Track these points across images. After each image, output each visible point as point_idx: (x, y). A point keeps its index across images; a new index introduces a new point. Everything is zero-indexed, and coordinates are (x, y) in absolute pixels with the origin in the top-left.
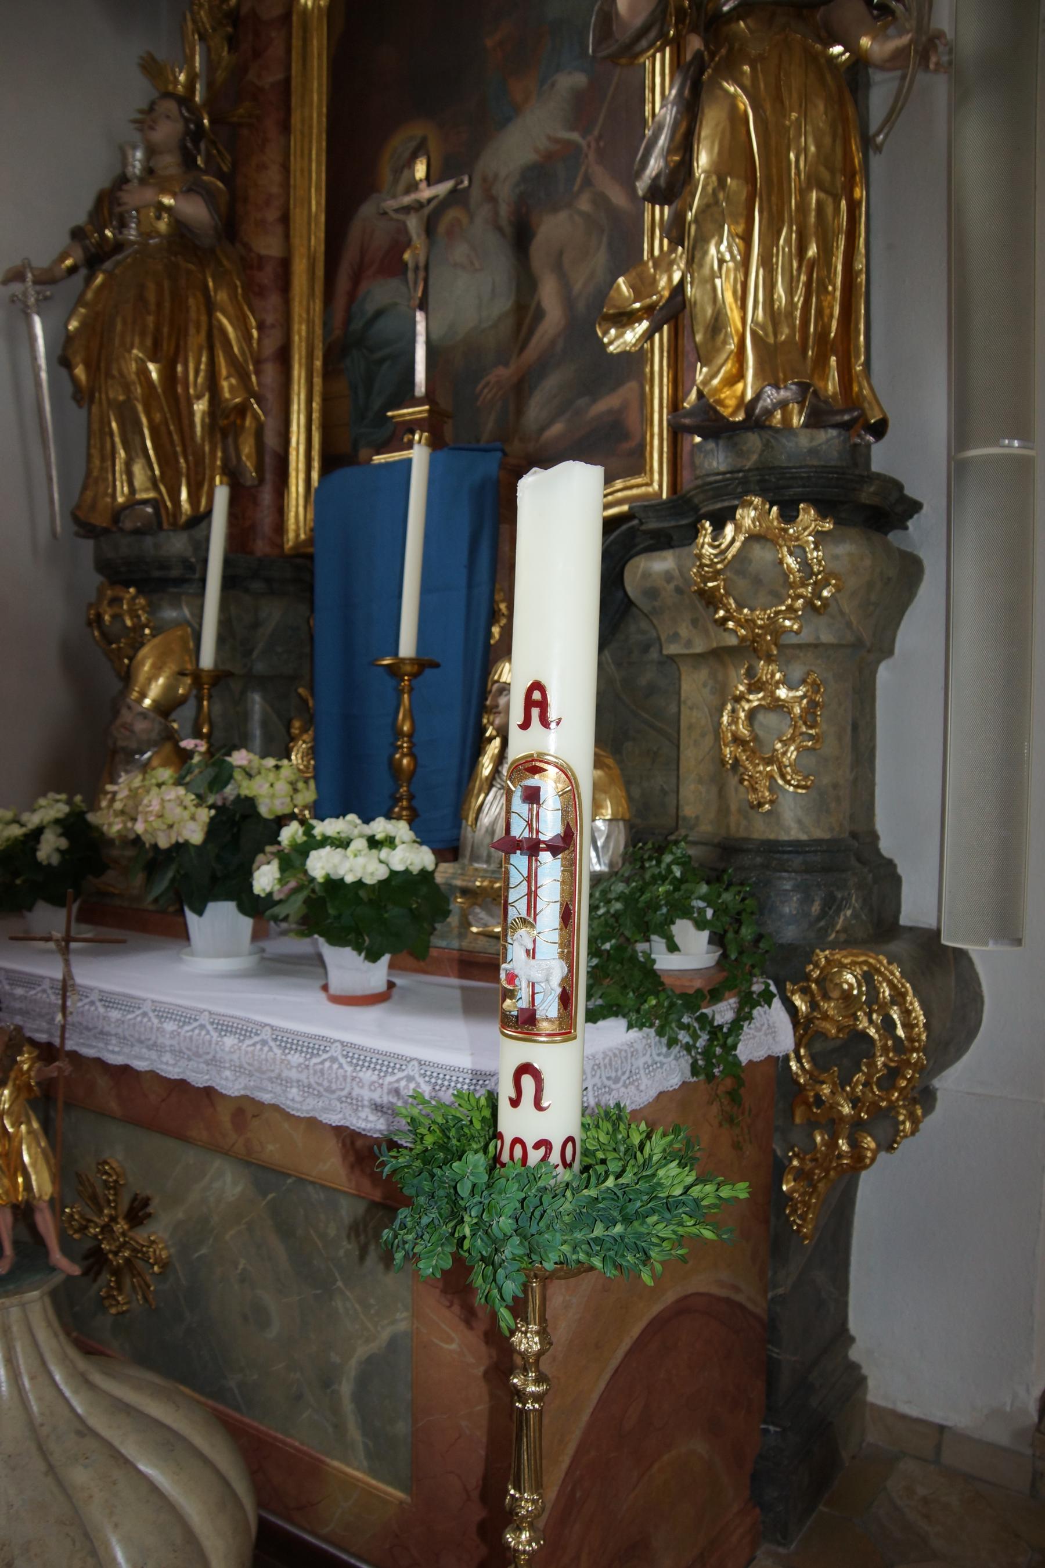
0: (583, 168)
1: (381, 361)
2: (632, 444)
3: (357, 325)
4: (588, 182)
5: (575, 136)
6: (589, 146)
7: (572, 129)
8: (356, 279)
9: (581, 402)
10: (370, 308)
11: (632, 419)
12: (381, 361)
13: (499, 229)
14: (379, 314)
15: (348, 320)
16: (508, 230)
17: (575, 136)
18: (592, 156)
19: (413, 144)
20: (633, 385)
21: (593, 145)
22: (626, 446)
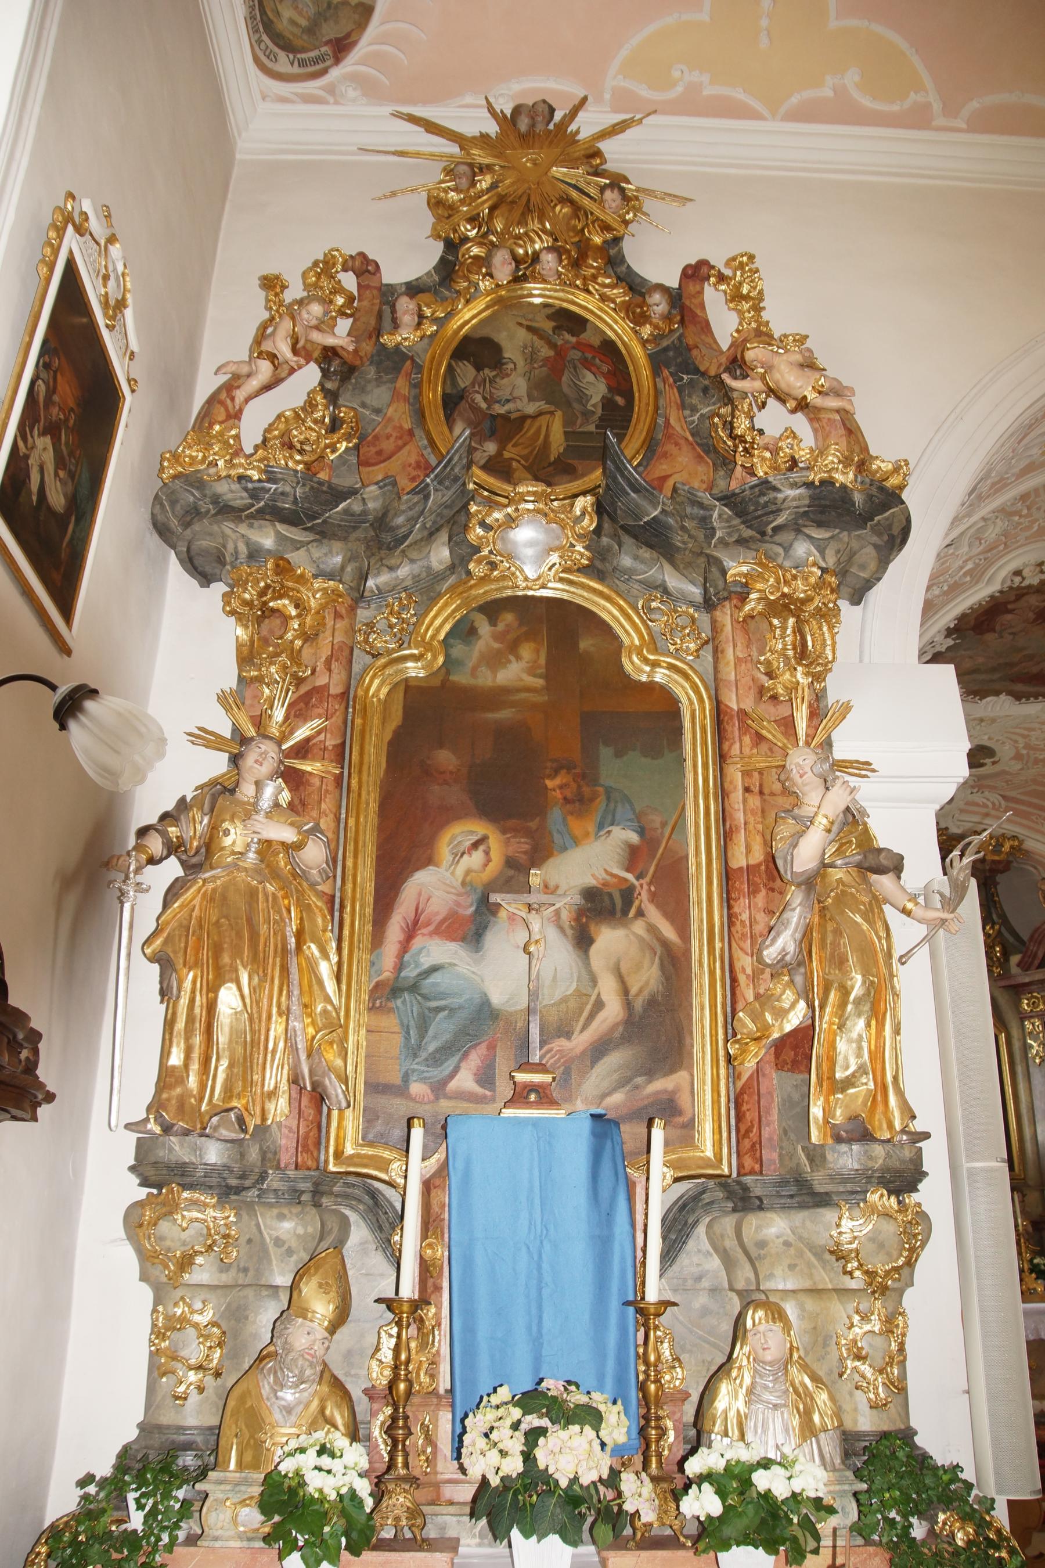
0: (636, 903)
1: (438, 1010)
2: (685, 1119)
3: (410, 973)
4: (640, 913)
5: (629, 876)
6: (642, 886)
7: (628, 870)
8: (411, 933)
9: (639, 1080)
10: (426, 962)
11: (683, 1100)
12: (438, 1010)
13: (561, 929)
14: (434, 969)
15: (400, 966)
16: (569, 932)
17: (629, 876)
18: (644, 895)
19: (475, 838)
20: (682, 1075)
21: (645, 887)
22: (680, 1120)
